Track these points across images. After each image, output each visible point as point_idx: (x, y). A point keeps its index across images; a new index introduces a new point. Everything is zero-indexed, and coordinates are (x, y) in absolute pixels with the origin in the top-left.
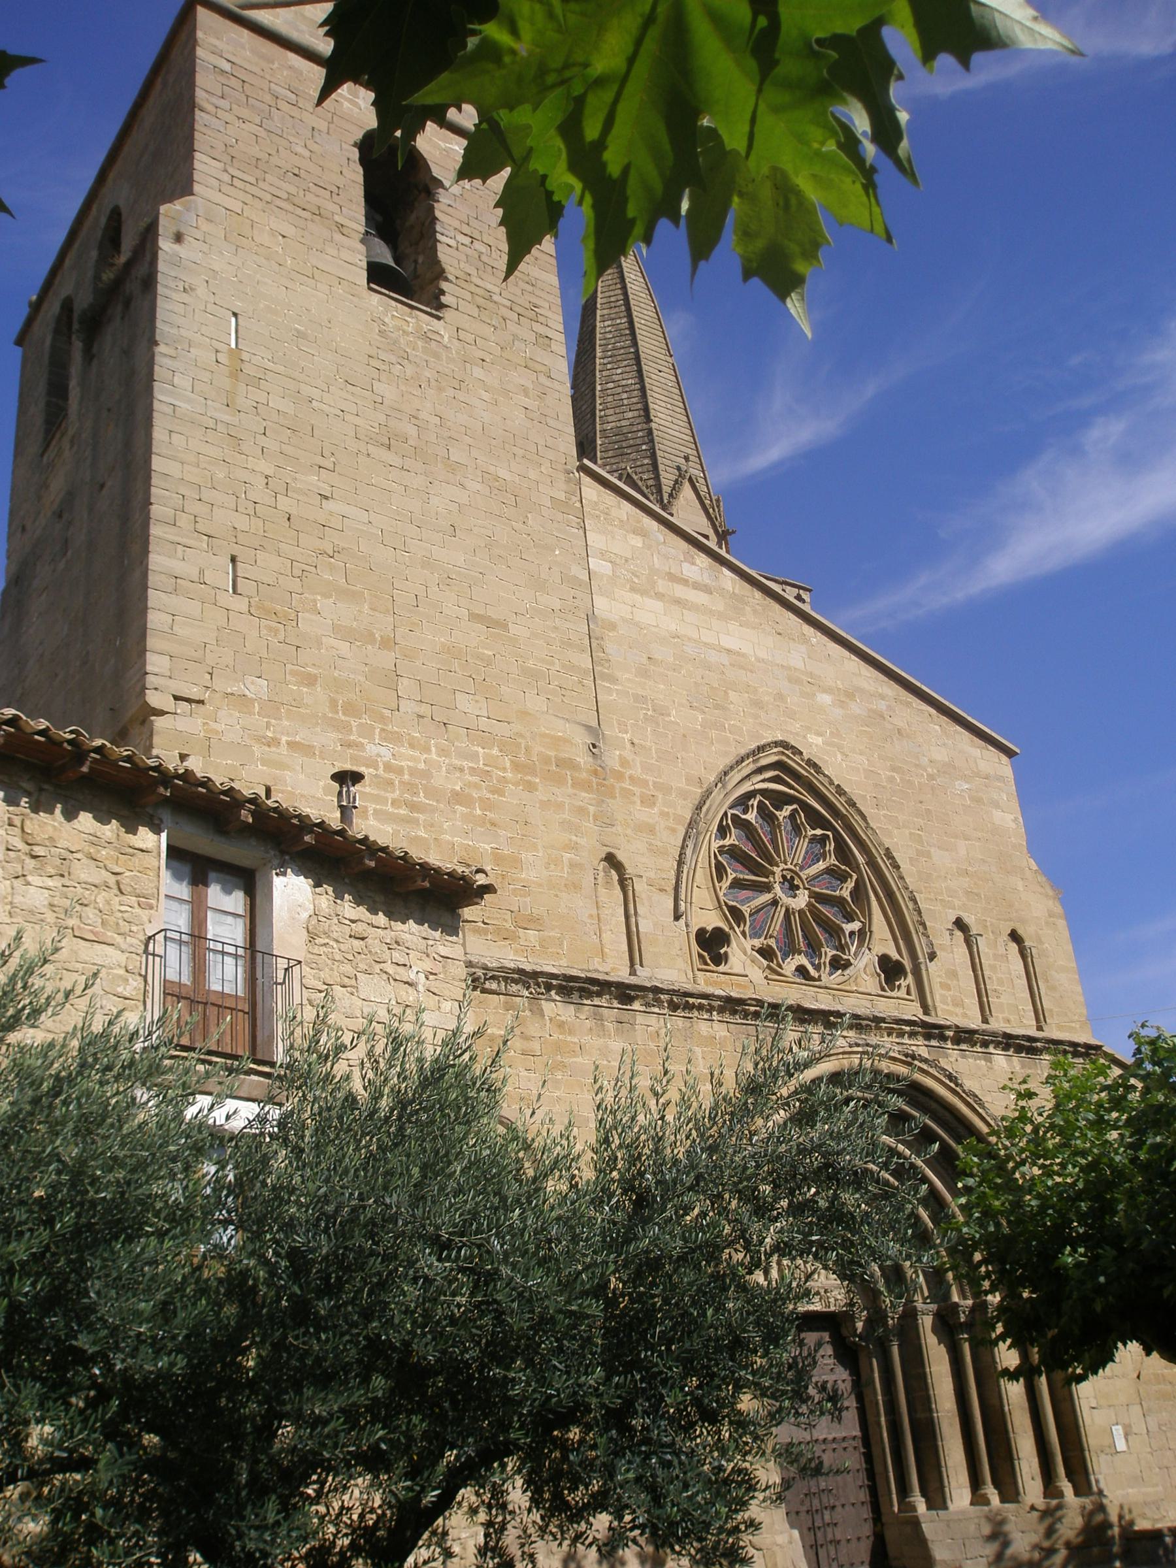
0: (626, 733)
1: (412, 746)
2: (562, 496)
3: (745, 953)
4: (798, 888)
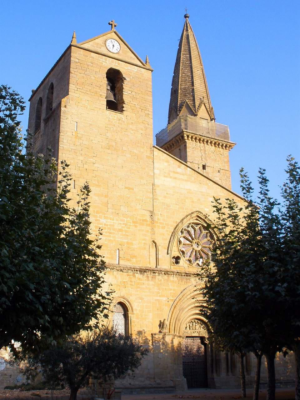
0: (159, 212)
1: (110, 219)
2: (148, 154)
3: (184, 261)
4: (199, 245)
